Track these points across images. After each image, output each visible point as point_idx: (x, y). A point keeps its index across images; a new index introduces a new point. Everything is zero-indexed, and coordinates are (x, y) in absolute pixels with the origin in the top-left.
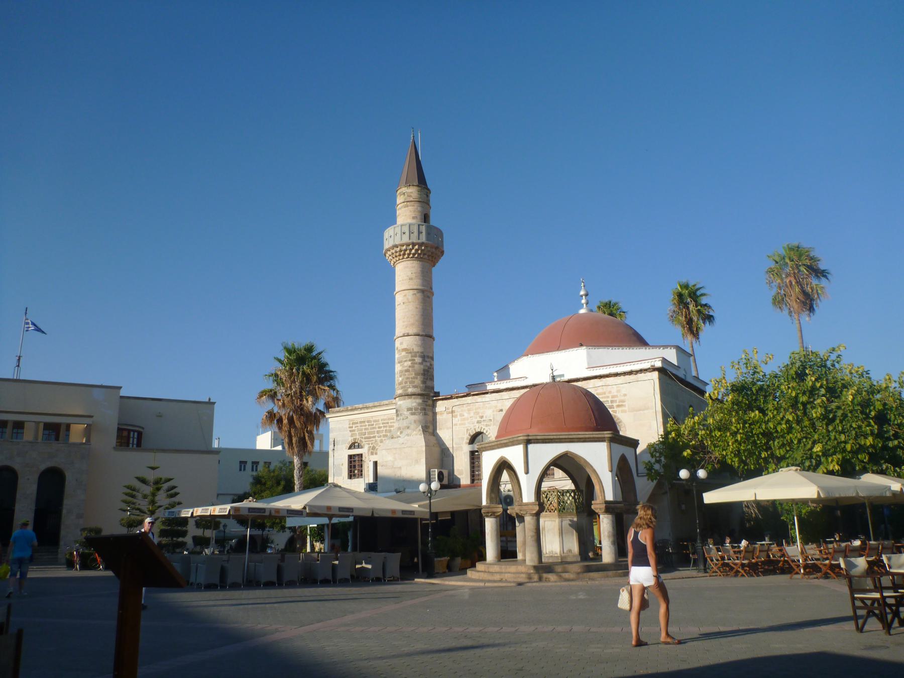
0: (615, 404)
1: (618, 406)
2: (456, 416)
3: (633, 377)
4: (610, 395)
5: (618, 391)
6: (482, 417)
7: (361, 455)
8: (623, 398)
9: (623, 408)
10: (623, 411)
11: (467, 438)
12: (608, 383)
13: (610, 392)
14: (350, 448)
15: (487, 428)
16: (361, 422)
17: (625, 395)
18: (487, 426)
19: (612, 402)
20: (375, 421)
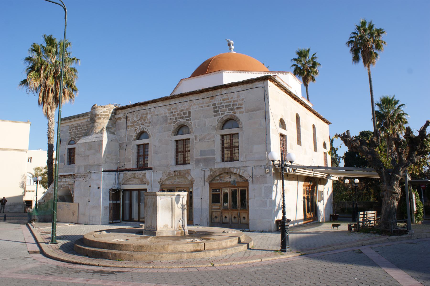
0: (235, 107)
1: (238, 108)
2: (129, 121)
3: (249, 86)
4: (232, 100)
5: (238, 97)
6: (145, 120)
7: (75, 148)
8: (241, 102)
9: (241, 110)
10: (240, 112)
11: (134, 134)
12: (230, 91)
13: (232, 98)
14: (69, 144)
15: (147, 128)
16: (76, 127)
17: (243, 99)
18: (148, 126)
19: (233, 105)
20: (83, 126)
